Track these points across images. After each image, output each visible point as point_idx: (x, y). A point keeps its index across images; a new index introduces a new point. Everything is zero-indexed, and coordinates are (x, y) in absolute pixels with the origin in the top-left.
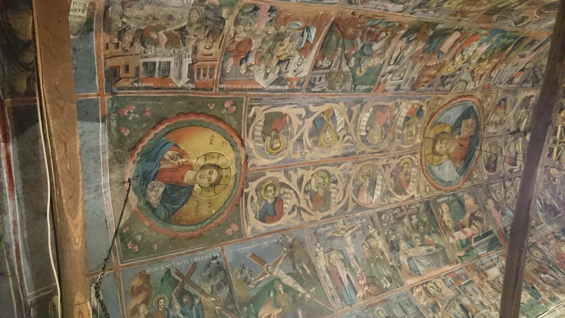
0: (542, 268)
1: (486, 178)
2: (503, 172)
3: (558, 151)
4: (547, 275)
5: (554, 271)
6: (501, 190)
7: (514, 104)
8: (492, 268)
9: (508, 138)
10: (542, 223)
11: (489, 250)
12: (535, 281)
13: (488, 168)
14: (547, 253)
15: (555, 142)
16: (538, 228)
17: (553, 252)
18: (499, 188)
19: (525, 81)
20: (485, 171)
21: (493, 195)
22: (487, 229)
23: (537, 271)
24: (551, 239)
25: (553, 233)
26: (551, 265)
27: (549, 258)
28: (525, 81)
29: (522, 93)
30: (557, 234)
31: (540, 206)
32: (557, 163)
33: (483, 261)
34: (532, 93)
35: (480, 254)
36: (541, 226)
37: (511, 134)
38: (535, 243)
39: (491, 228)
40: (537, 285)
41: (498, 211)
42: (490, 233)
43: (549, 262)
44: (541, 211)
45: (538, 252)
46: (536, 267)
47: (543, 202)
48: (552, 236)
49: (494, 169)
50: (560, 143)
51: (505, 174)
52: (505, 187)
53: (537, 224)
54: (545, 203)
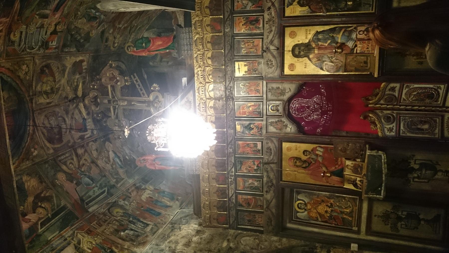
0: (122, 225)
1: (52, 151)
2: (72, 141)
3: (114, 110)
4: (127, 231)
5: (134, 224)
6: (72, 159)
7: (64, 71)
8: (65, 250)
9: (69, 106)
10: (123, 179)
11: (61, 229)
12: (114, 243)
13: (51, 141)
14: (127, 208)
15: (109, 101)
16: (119, 185)
17: (134, 204)
18: (69, 158)
19: (65, 46)
20: (48, 145)
21: (64, 167)
22: (58, 206)
23: (117, 231)
24: (132, 191)
25: (135, 185)
26: (131, 219)
27: (130, 212)
28: (65, 46)
29: (68, 58)
30: (138, 185)
31: (120, 163)
32: (117, 121)
33: (54, 246)
34: (81, 58)
35: (49, 239)
36: (122, 182)
37: (70, 101)
38: (115, 202)
39: (63, 203)
40: (117, 247)
41: (72, 182)
42: (64, 208)
43: (130, 216)
44: (121, 168)
45: (119, 210)
46: (116, 227)
47: (122, 160)
48: (133, 188)
49: (60, 140)
50: (114, 102)
51: (75, 142)
52: (77, 155)
53: (117, 182)
54: (125, 159)
